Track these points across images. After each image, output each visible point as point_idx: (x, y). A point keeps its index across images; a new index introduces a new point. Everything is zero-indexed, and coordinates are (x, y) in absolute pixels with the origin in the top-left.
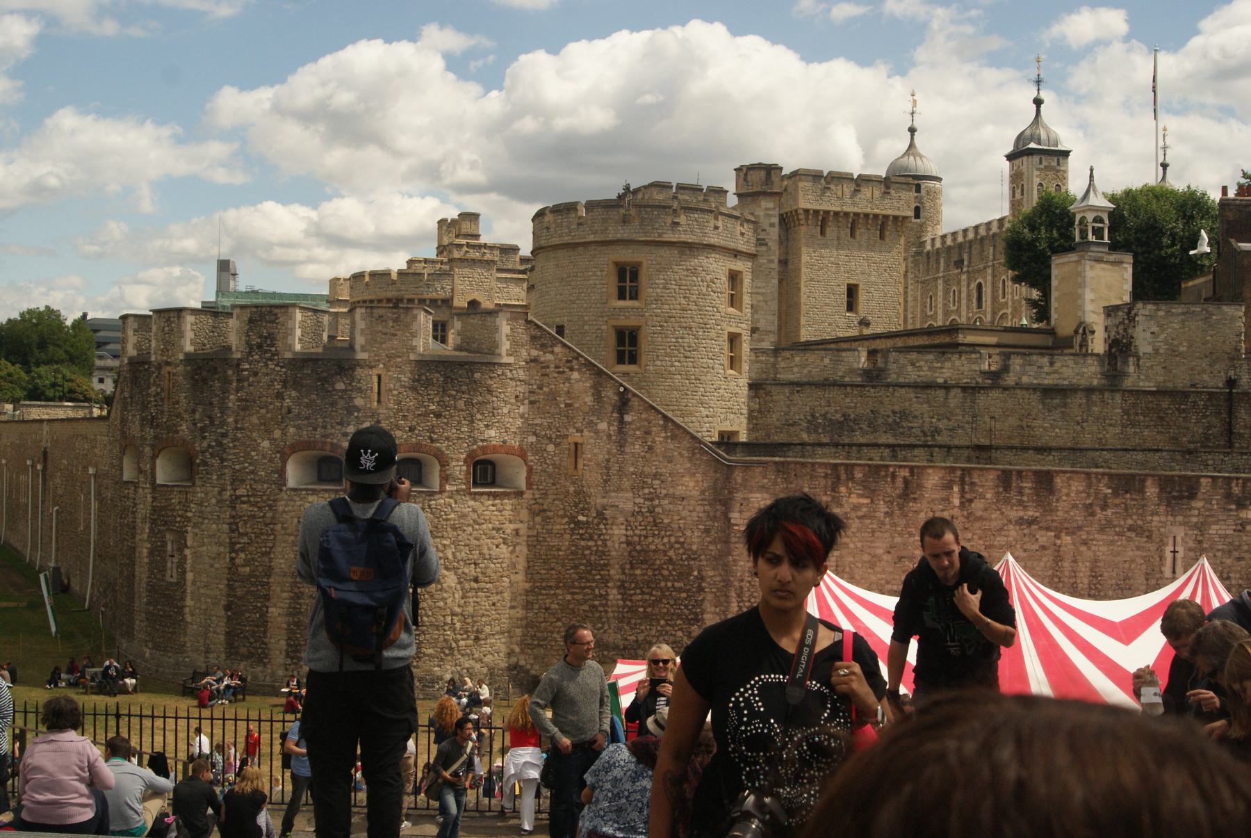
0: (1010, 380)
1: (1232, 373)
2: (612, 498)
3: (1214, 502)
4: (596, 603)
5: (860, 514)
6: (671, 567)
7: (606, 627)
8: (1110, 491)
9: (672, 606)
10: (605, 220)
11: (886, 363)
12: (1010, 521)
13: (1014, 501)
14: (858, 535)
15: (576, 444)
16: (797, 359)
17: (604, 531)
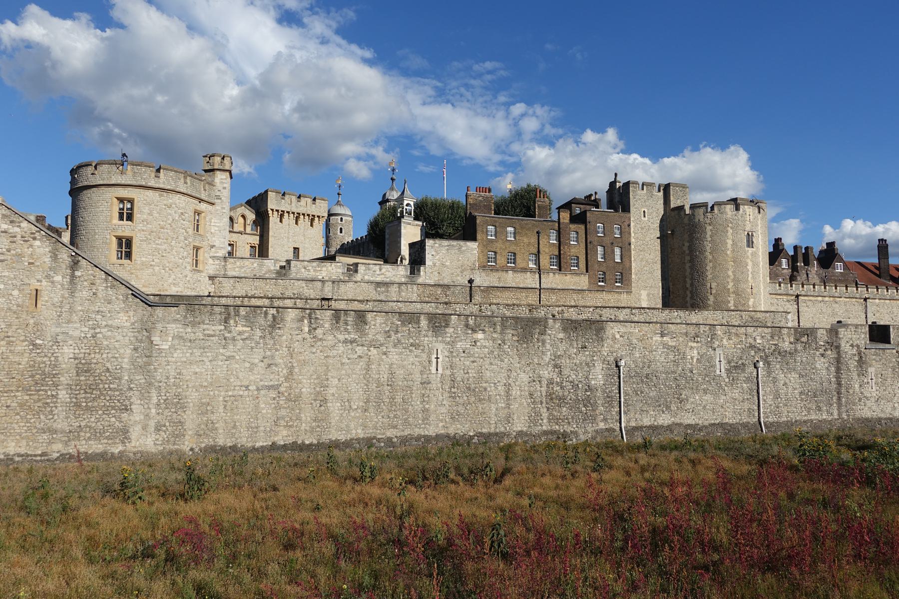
0: (358, 277)
1: (472, 276)
2: (63, 327)
3: (459, 329)
4: (48, 401)
5: (243, 337)
6: (108, 374)
7: (56, 417)
8: (400, 323)
9: (108, 401)
10: (109, 172)
11: (290, 267)
12: (339, 341)
13: (342, 329)
14: (242, 350)
15: (37, 290)
16: (238, 263)
17: (57, 351)
